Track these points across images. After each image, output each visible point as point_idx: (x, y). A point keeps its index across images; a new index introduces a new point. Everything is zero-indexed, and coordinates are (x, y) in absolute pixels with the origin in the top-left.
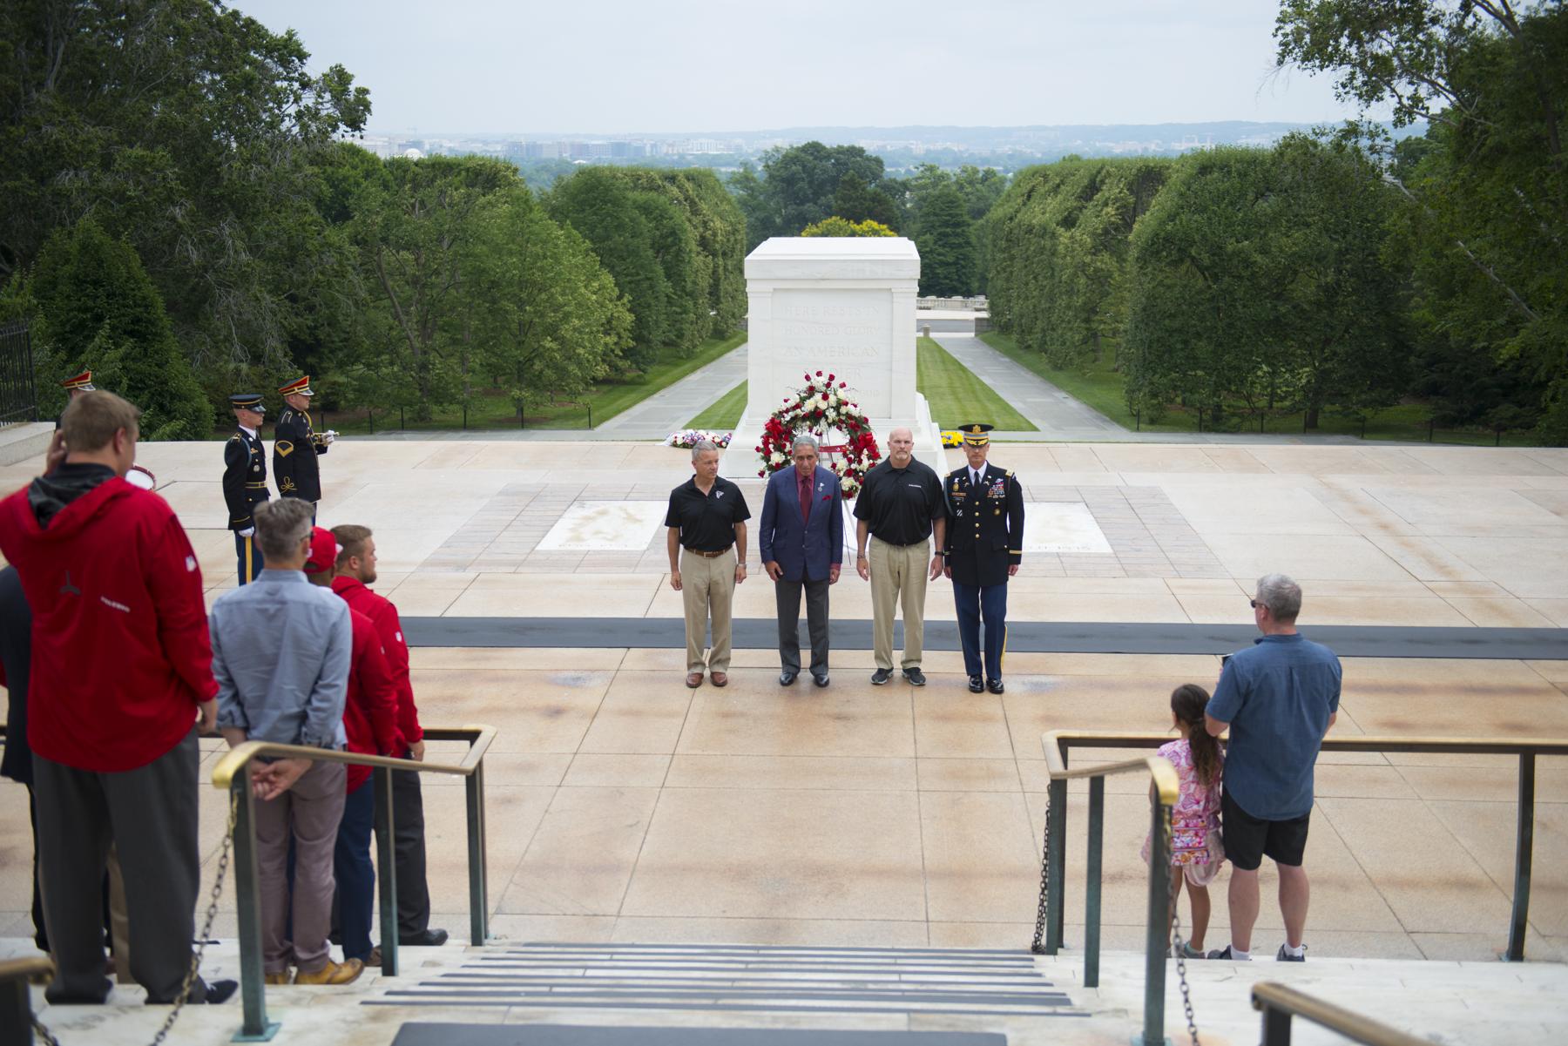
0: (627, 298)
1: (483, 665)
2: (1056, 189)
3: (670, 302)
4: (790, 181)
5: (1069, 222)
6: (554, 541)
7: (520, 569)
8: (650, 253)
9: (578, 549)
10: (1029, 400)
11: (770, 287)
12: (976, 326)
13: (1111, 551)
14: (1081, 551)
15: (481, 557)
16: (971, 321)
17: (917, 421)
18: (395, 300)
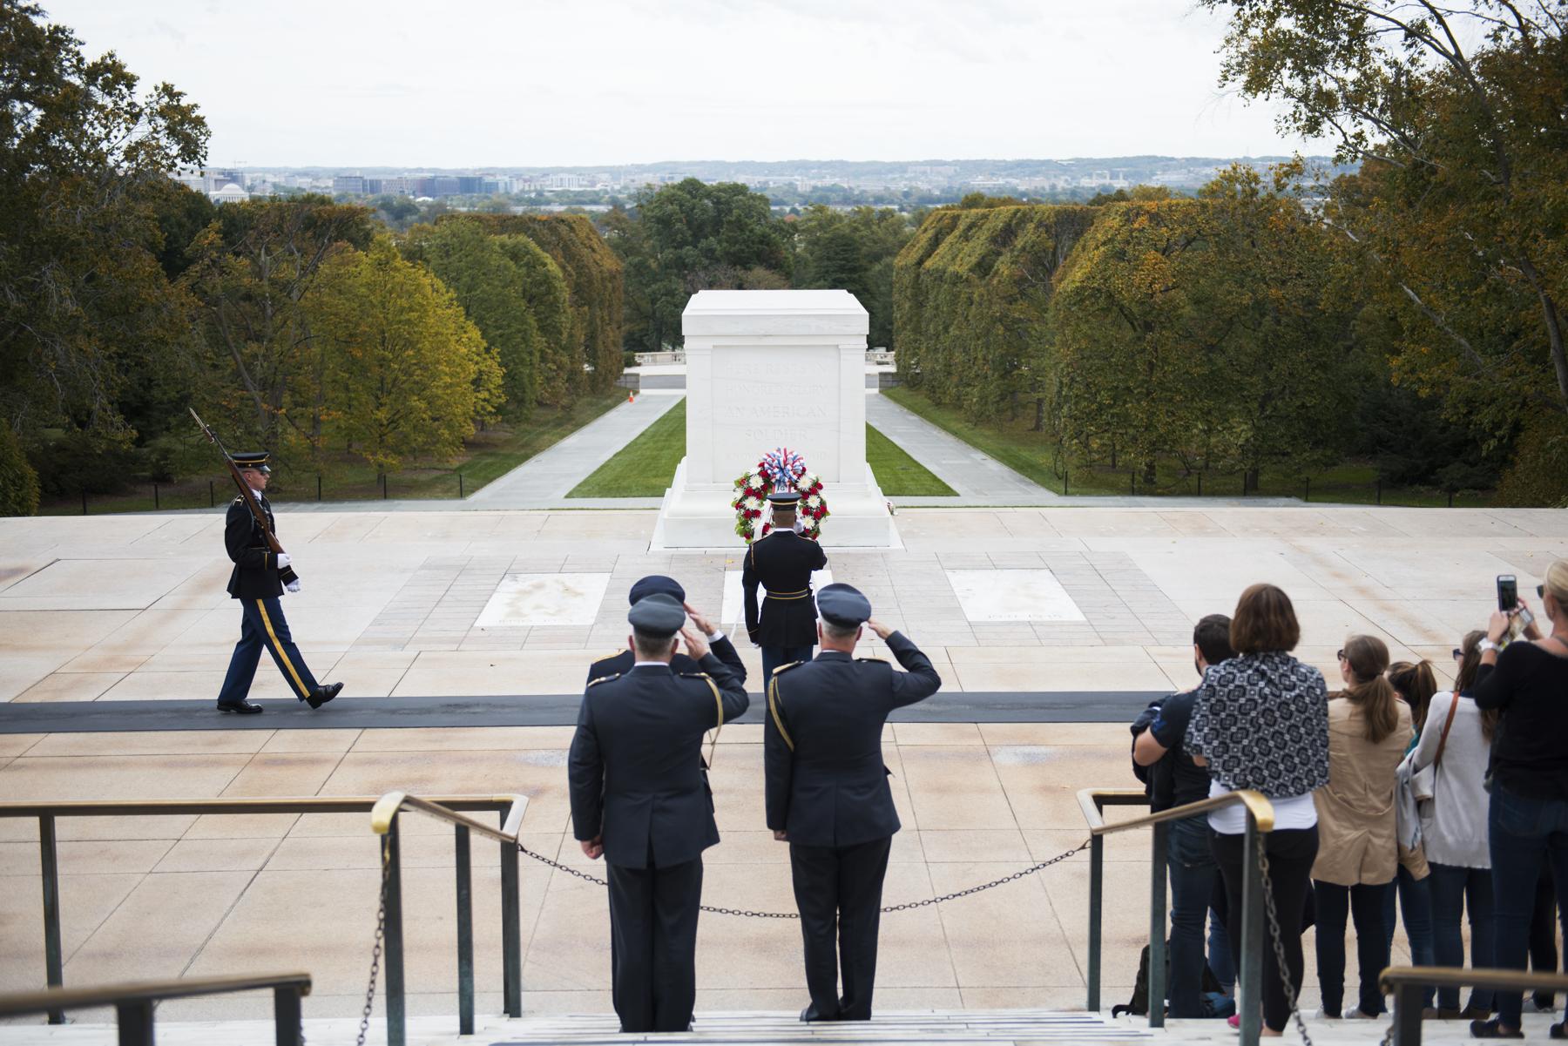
0: (495, 351)
1: (446, 746)
2: (966, 237)
3: (543, 359)
4: (665, 222)
5: (984, 267)
6: (493, 615)
7: (462, 647)
8: (523, 303)
9: (521, 624)
10: (944, 462)
11: (709, 344)
12: (880, 381)
13: (1085, 619)
14: (1054, 619)
15: (419, 635)
16: (874, 376)
17: (867, 485)
18: (238, 356)
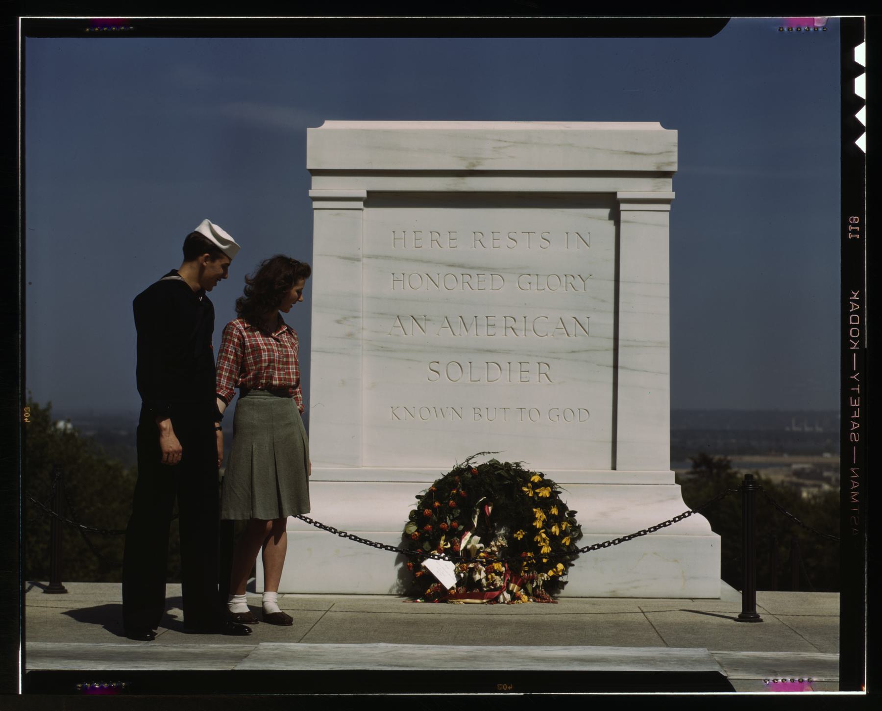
11: (360, 187)
